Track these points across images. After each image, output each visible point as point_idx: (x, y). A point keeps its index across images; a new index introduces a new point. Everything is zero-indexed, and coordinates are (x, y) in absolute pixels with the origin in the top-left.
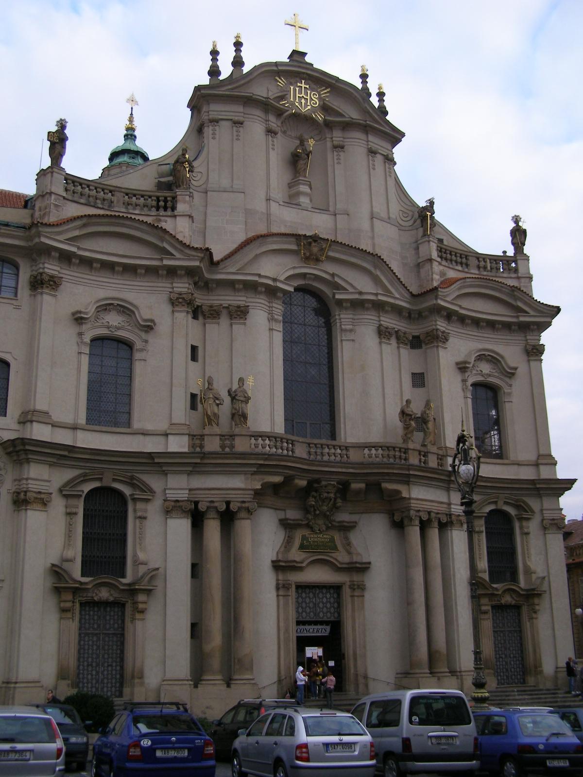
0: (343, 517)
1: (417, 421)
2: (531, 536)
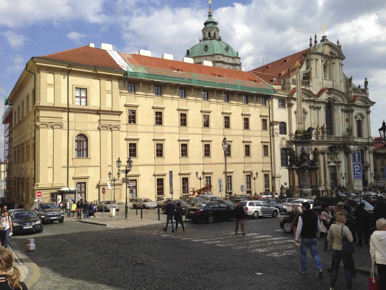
0: (336, 152)
1: (350, 130)
2: (367, 155)
